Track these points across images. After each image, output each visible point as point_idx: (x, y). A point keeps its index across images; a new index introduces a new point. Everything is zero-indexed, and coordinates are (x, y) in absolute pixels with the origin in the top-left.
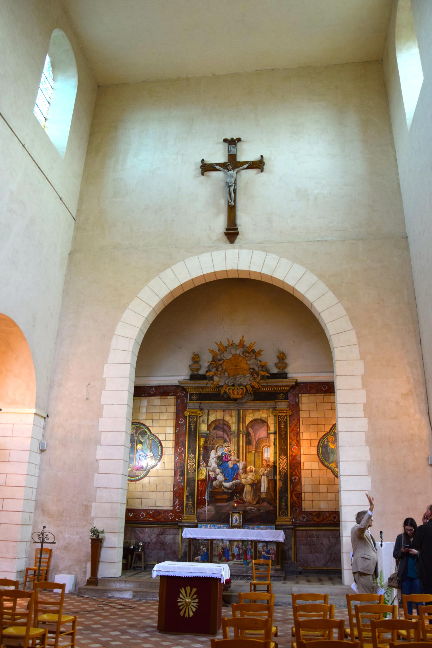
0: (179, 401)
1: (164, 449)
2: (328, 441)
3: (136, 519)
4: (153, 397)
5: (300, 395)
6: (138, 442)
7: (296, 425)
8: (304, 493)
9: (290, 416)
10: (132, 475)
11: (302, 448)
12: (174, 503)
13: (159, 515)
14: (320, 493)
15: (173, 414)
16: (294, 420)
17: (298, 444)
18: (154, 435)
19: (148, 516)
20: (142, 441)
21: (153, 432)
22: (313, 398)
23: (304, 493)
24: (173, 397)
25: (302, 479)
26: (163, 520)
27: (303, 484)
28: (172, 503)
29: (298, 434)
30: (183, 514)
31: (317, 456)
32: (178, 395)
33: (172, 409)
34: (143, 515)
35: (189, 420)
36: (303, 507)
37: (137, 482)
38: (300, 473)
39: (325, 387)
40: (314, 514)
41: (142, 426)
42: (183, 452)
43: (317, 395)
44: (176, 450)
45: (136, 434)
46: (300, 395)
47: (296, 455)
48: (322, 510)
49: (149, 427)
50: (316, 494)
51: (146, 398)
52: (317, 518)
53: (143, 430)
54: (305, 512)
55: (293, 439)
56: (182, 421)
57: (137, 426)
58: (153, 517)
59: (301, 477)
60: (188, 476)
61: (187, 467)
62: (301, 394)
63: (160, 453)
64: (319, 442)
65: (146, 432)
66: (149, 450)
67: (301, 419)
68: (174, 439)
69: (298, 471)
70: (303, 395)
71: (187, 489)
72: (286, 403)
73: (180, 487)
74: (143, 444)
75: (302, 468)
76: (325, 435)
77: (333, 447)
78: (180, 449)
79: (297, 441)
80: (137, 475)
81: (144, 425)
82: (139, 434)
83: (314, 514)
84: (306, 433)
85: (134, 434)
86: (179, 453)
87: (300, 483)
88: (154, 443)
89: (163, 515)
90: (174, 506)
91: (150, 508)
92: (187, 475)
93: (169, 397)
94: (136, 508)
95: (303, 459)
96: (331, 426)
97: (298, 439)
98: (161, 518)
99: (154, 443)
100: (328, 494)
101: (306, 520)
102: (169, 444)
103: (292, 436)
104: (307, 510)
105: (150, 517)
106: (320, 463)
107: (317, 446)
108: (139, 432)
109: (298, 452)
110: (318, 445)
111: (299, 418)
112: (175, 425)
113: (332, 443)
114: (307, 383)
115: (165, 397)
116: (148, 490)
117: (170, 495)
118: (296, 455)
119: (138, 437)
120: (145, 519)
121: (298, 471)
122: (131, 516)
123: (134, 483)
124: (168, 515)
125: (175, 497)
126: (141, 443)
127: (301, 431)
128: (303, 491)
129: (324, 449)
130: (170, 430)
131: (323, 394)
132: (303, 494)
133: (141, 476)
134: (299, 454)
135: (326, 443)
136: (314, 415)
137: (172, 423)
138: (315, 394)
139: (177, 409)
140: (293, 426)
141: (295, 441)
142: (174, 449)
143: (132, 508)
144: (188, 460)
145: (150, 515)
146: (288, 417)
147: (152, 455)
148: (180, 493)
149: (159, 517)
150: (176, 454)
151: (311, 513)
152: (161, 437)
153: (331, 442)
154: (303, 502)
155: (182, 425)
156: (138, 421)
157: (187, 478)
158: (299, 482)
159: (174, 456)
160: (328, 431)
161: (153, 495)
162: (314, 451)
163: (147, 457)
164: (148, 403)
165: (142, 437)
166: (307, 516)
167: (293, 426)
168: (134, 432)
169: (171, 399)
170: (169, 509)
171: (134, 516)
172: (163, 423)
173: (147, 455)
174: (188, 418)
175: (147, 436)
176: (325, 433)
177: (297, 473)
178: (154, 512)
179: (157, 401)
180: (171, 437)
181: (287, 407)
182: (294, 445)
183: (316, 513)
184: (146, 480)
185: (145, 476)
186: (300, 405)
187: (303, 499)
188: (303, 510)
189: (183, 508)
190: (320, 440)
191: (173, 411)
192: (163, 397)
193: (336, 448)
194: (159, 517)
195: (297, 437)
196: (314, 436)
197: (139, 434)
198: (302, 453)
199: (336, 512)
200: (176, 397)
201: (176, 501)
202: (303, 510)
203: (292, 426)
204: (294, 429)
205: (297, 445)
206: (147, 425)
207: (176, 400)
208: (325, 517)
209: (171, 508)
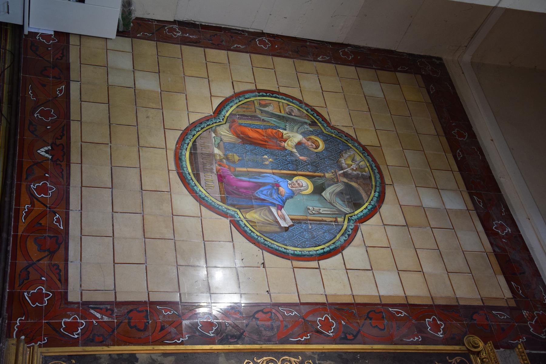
0: (505, 316)
1: (314, 264)
3: (25, 167)
4: (480, 228)
6: (320, 182)
10: (200, 160)
12: (98, 305)
13: (41, 249)
15: (450, 294)
18: (356, 230)
19: (39, 208)
20: (326, 194)
21: (363, 227)
24: (508, 294)
26: (21, 263)
28: (99, 297)
30: (45, 345)
32: (525, 313)
33: (465, 292)
34: (43, 190)
35: (452, 355)
37: (174, 176)
41: (374, 195)
42: (318, 335)
44: (319, 308)
45: (345, 175)
49: (377, 216)
51: (471, 206)
53: (364, 195)
56: (437, 328)
57: (370, 177)
58: (35, 226)
60: (222, 359)
61: (261, 353)
63: (298, 250)
65: (357, 205)
66: (299, 214)
68: (358, 301)
71: (166, 355)
73: (173, 330)
74: (316, 197)
78: (327, 325)
80: (202, 175)
81: (381, 199)
82: (347, 185)
85: (342, 169)
86: (310, 318)
88: (329, 231)
89: (45, 262)
90: (85, 307)
91: (74, 217)
92: (228, 354)
93: (502, 279)
94: (75, 169)
98: (27, 256)
99: (329, 231)
102: (334, 281)
105: (33, 215)
108: (353, 184)
112: (411, 302)
115: (498, 268)
116: (147, 210)
117: (132, 288)
119: (334, 181)
120: (25, 197)
122: (42, 152)
123: (172, 166)
124: (42, 283)
125: (124, 310)
126: (318, 190)
130: (387, 286)
133: (199, 188)
137: (416, 291)
139: (471, 310)
142: (323, 300)
143: (74, 157)
144: (294, 354)
145: (43, 215)
147: (283, 224)
148: (146, 329)
149: (32, 247)
150: (304, 310)
152: (354, 254)
155: (421, 330)
156: (387, 181)
157: (217, 353)
159: (295, 300)
161: (127, 228)
163: (274, 210)
164: (456, 212)
165: (340, 194)
168: (349, 170)
169: (499, 290)
170: (70, 288)
171: (40, 163)
172: (406, 259)
173: (280, 208)
174: (457, 347)
175: (346, 209)
178: (56, 230)
179: (473, 239)
180: (365, 290)
184: (185, 203)
185: (201, 200)
189: (75, 343)
191: (459, 294)
192: (494, 259)
194: (32, 247)
197: (347, 185)
200: (513, 304)
201: (109, 312)
206: (385, 209)
207: (503, 304)
209: (73, 296)
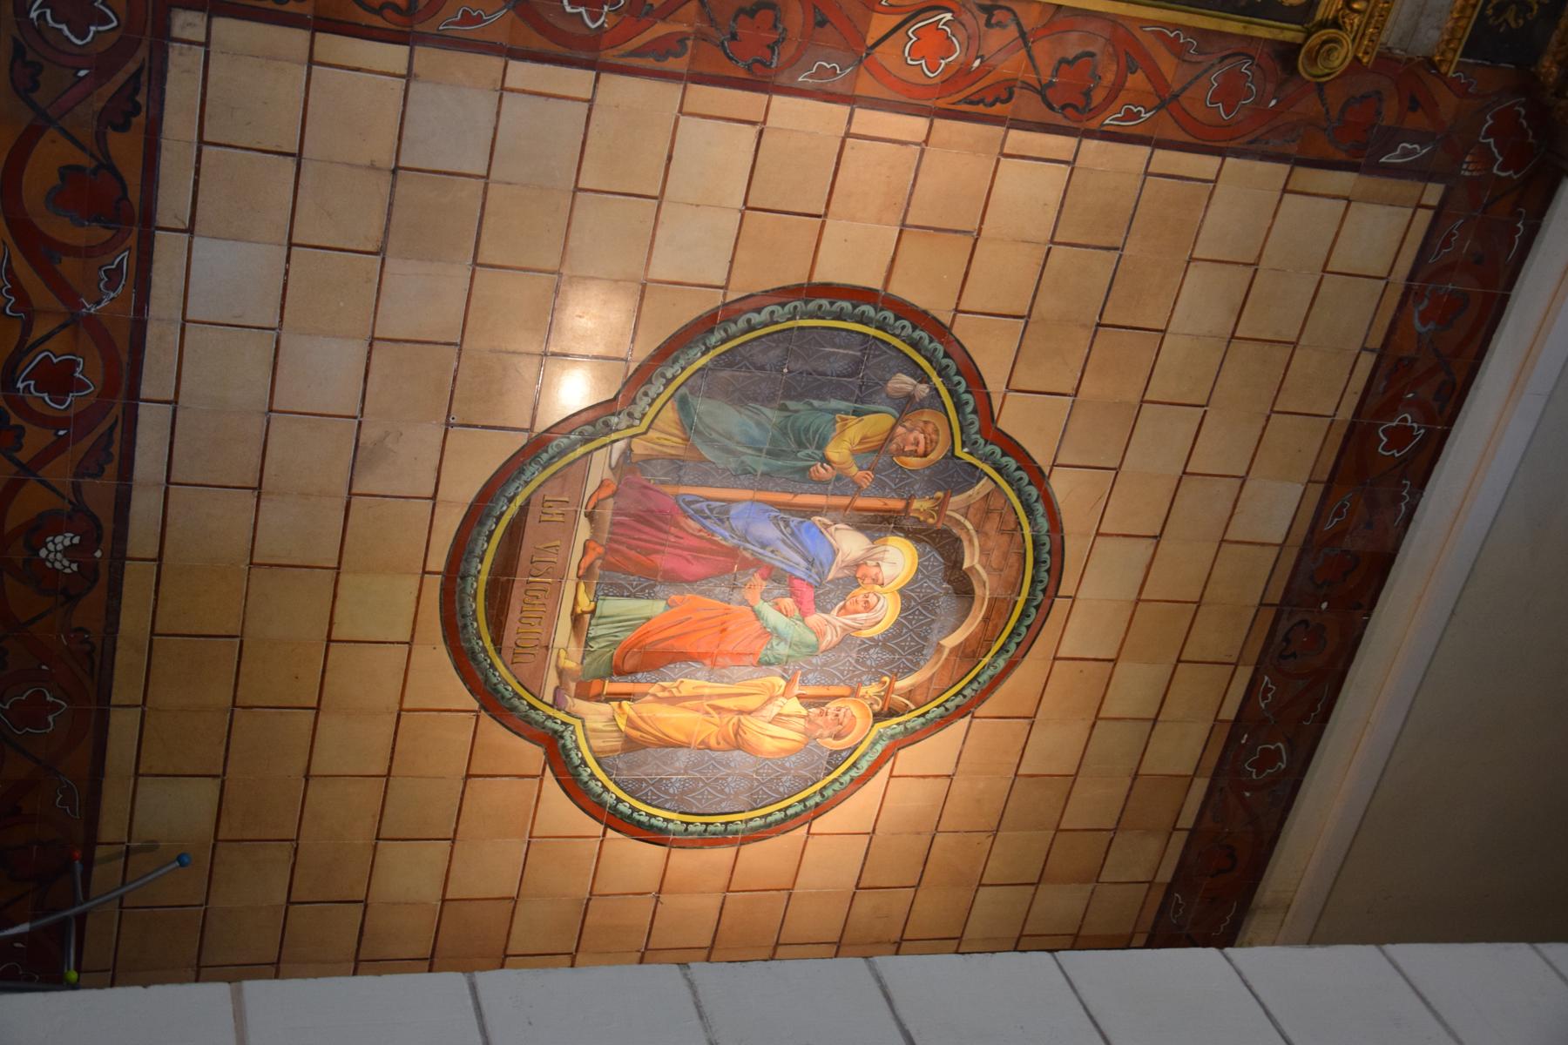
2: (906, 406)
5: (1434, 193)
7: (1166, 101)
8: (409, 76)
9: (1287, 54)
11: (915, 126)
14: (381, 252)
16: (1229, 93)
17: (972, 99)
22: (1352, 322)
23: (409, 76)
25: (577, 81)
27: (522, 73)
29: (1070, 109)
31: (794, 275)
36: (228, 29)
38: (652, 63)
39: (1400, 436)
40: (124, 148)
43: (1367, 361)
46: (1434, 193)
47: (860, 53)
48: (167, 249)
50: (378, 221)
52: (70, 173)
54: (163, 35)
55: (1041, 49)
59: (599, 67)
62: (1439, 212)
64: (920, 318)
67: (1205, 165)
69: (662, 48)
70: (1424, 217)
72: (1430, 37)
75: (703, 96)
76: (976, 380)
77: (838, 451)
79: (1006, 91)
83: (124, 148)
84: (1054, 196)
87: (538, 43)
95: (801, 120)
96: (1042, 458)
97: (1028, 105)
100: (359, 349)
101: (39, 30)
103: (1073, 45)
104: (182, 70)
106: (716, 299)
107: (898, 289)
109: (881, 74)
110: (904, 310)
111: (1222, 153)
113: (878, 449)
114: (1511, 284)
118: (860, 53)
121: (662, 48)
127: (1090, 145)
128: (427, 57)
129: (838, 358)
131: (1346, 414)
132: (393, 56)
134: (867, 85)
135: (902, 382)
136: (1201, 306)
138: (1376, 341)
140: (1167, 64)
141: (1011, 65)
146: (1289, 33)
151: (137, 108)
153: (890, 436)
154: (297, 39)
158: (543, 28)
160: (1004, 424)
162: (852, 256)
166: (104, 64)
167: (1167, 64)
176: (995, 383)
177: (660, 29)
181: (1390, 36)
182: (972, 41)
183: (133, 179)
186: (1343, 181)
187: (333, 46)
188: (188, 24)
190: (940, 330)
193: (822, 471)
195: (1043, 91)
196: (1002, 275)
198: (867, 120)
199: (134, 394)
202: (188, 24)
203: (1177, 50)
204: (1137, 80)
205: (961, 74)
208: (68, 267)
